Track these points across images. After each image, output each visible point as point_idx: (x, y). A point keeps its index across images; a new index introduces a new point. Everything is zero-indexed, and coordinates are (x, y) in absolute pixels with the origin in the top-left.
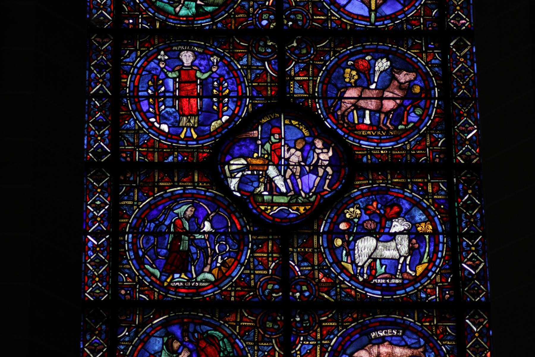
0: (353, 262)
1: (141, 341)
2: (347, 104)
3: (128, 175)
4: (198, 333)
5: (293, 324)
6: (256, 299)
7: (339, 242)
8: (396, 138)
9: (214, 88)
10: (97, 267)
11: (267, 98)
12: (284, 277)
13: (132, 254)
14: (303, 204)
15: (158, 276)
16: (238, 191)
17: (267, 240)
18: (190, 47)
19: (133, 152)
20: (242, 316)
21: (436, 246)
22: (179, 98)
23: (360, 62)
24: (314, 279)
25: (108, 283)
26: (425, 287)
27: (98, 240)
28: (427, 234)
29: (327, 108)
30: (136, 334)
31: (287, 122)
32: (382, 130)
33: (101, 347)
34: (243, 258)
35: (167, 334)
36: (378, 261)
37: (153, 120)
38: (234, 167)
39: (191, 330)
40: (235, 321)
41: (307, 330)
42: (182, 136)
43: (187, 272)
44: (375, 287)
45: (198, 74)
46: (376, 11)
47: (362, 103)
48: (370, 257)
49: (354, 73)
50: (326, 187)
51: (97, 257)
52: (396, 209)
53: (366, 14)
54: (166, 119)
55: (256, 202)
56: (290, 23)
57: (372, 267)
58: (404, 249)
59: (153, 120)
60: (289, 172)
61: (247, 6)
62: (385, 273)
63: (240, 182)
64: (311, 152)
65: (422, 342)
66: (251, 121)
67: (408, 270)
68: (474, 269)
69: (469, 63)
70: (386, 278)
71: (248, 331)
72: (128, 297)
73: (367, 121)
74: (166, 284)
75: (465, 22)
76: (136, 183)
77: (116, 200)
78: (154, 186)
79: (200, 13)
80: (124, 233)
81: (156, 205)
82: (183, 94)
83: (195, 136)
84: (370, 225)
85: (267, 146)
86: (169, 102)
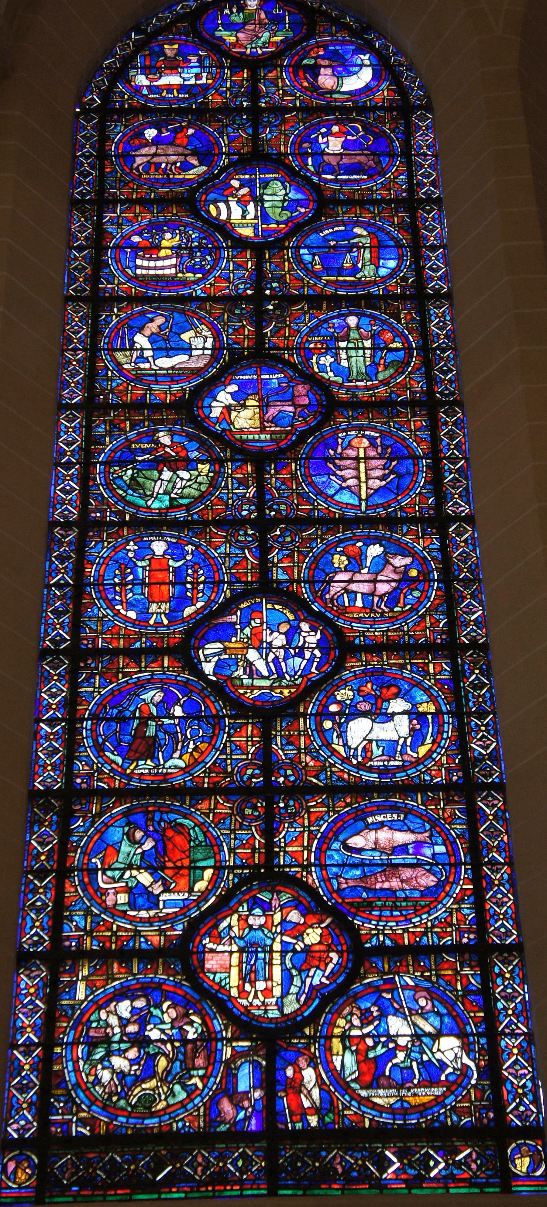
0: (345, 745)
1: (97, 831)
2: (335, 588)
3: (89, 662)
4: (165, 821)
5: (276, 811)
6: (233, 786)
7: (328, 724)
8: (392, 620)
9: (188, 575)
10: (50, 755)
11: (246, 583)
12: (266, 760)
13: (90, 741)
14: (287, 687)
15: (120, 763)
16: (215, 674)
17: (247, 724)
18: (161, 537)
19: (95, 640)
20: (217, 803)
22: (149, 585)
23: (350, 548)
24: (301, 763)
25: (62, 772)
26: (429, 769)
27: (52, 727)
28: (429, 713)
29: (314, 592)
30: (93, 823)
31: (269, 606)
32: (376, 612)
33: (51, 839)
34: (219, 742)
36: (374, 743)
37: (118, 607)
38: (207, 652)
39: (157, 818)
40: (209, 809)
41: (293, 816)
42: (152, 622)
43: (153, 758)
44: (371, 769)
45: (171, 563)
46: (367, 500)
47: (353, 587)
48: (364, 739)
49: (344, 558)
50: (313, 670)
51: (51, 745)
53: (357, 503)
54: (133, 605)
55: (234, 686)
56: (273, 513)
58: (404, 730)
59: (118, 607)
60: (271, 656)
61: (225, 498)
62: (383, 755)
63: (217, 666)
64: (297, 635)
65: (428, 826)
66: (229, 606)
67: (409, 752)
68: (486, 748)
69: (471, 547)
70: (384, 761)
71: (224, 819)
72: (84, 786)
73: (359, 603)
74: (128, 771)
75: (464, 509)
76: (97, 668)
77: (74, 686)
78: (119, 672)
79: (173, 505)
82: (153, 581)
83: (166, 622)
84: (364, 707)
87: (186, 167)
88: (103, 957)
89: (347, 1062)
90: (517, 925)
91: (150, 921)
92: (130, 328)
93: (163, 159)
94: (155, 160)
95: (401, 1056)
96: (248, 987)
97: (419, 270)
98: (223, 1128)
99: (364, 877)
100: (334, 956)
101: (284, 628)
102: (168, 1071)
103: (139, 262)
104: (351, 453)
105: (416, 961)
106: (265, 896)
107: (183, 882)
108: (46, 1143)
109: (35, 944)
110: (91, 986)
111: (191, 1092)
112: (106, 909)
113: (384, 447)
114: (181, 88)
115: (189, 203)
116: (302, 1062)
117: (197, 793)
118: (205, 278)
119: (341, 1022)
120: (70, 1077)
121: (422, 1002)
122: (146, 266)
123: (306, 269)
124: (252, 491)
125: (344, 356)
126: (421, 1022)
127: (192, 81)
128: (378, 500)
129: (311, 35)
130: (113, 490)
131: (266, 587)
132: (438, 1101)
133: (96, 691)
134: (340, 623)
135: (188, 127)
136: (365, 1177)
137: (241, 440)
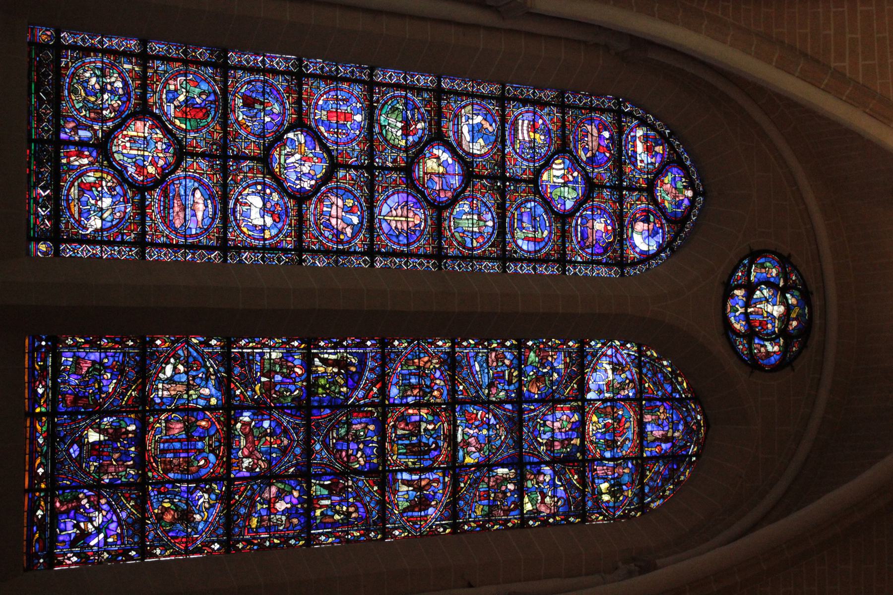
0: (248, 194)
2: (334, 199)
7: (259, 187)
8: (316, 224)
10: (246, 60)
11: (337, 157)
12: (240, 157)
21: (258, 239)
22: (337, 112)
29: (332, 188)
35: (210, 93)
41: (212, 167)
43: (244, 106)
44: (235, 205)
47: (334, 207)
52: (277, 220)
57: (246, 204)
66: (324, 148)
68: (246, 258)
73: (325, 209)
75: (378, 265)
79: (382, 127)
80: (264, 75)
81: (279, 94)
84: (268, 206)
85: (311, 155)
86: (335, 106)
87: (586, 150)
88: (143, 78)
89: (91, 178)
90: (154, 260)
91: (161, 99)
92: (486, 115)
93: (590, 139)
94: (590, 135)
95: (93, 202)
96: (127, 139)
97: (521, 260)
98: (62, 122)
99: (179, 195)
100: (141, 178)
101: (312, 173)
102: (89, 101)
103: (526, 122)
104: (411, 214)
105: (138, 214)
106: (171, 150)
107: (180, 115)
108: (59, 48)
109: (151, 48)
110: (130, 71)
111: (79, 111)
112: (167, 80)
113: (414, 231)
114: (635, 152)
115: (563, 148)
116: (91, 159)
117: (224, 124)
118: (516, 153)
119: (109, 178)
120: (87, 60)
121: (118, 214)
122: (523, 127)
123: (522, 204)
124: (390, 165)
125: (469, 217)
126: (108, 212)
127: (639, 158)
128: (384, 225)
129: (667, 220)
130: (391, 99)
131: (334, 166)
132: (72, 216)
133: (280, 83)
134: (314, 199)
135: (610, 153)
136: (38, 181)
137: (418, 163)
